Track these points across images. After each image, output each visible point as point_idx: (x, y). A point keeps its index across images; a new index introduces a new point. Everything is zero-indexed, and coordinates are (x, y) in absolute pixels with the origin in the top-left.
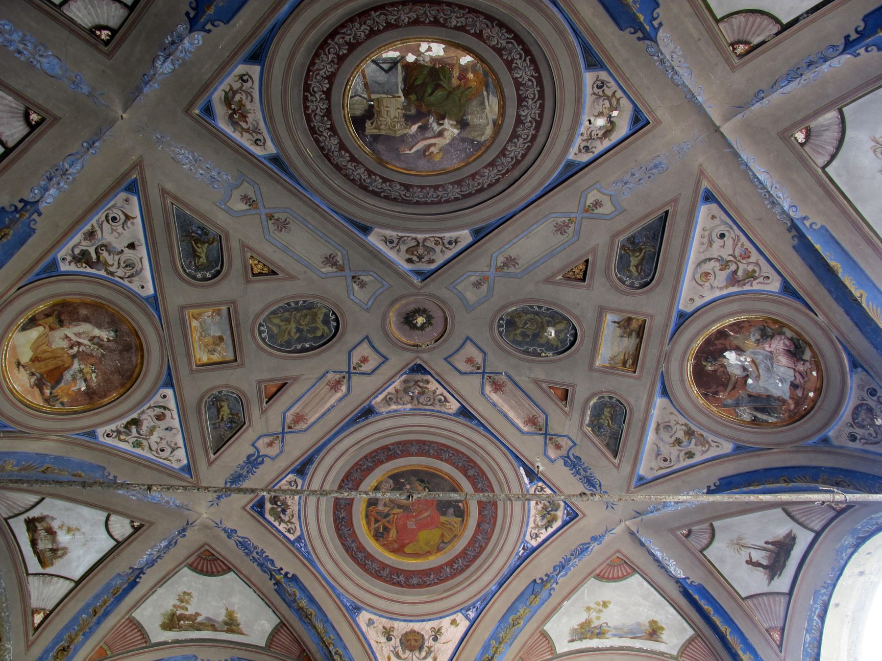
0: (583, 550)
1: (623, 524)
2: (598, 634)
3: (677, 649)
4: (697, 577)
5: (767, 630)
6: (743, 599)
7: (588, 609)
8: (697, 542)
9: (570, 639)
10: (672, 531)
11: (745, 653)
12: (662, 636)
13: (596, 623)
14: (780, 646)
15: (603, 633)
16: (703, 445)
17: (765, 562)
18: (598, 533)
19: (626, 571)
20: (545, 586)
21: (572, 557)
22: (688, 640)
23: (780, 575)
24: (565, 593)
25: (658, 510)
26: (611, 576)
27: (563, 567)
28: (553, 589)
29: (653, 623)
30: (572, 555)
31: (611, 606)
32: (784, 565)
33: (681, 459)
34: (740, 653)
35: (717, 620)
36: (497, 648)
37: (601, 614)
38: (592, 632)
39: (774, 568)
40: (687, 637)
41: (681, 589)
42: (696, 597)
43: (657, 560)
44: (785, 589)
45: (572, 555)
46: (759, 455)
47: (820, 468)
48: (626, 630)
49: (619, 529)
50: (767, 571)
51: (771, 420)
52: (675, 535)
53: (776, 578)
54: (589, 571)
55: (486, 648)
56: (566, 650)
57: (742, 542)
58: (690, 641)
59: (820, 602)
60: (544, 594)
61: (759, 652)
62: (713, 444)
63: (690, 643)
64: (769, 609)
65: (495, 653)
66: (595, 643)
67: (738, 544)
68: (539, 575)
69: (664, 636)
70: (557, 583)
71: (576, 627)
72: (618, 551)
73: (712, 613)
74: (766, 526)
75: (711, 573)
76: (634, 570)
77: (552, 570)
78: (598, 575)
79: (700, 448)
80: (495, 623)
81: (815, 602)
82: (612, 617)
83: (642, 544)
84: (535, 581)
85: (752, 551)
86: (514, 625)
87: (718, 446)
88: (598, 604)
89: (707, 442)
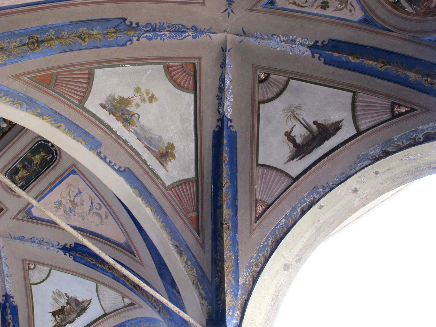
0: (179, 30)
1: (224, 35)
2: (126, 120)
3: (172, 181)
4: (238, 124)
5: (256, 201)
6: (258, 165)
7: (138, 90)
8: (264, 92)
9: (104, 102)
10: (255, 68)
11: (228, 208)
12: (169, 162)
13: (132, 108)
14: (257, 219)
15: (130, 123)
16: (341, 4)
17: (299, 141)
18: (201, 26)
19: (189, 84)
20: (129, 30)
21: (167, 29)
22: (186, 179)
23: (300, 159)
24: (136, 55)
25: (264, 39)
26: (175, 78)
27: (154, 30)
28: (131, 40)
29: (171, 146)
30: (169, 27)
31: (154, 104)
32: (311, 151)
33: (316, 5)
34: (225, 206)
35: (226, 170)
36: (52, 39)
37: (142, 104)
38: (123, 114)
39: (300, 150)
40: (187, 177)
41: (217, 129)
42: (225, 141)
43: (221, 89)
44: (294, 174)
45: (169, 27)
46: (378, 33)
47: (420, 60)
48: (148, 135)
49: (218, 37)
50: (295, 149)
51: (409, 9)
52: (254, 73)
53: (296, 159)
54: (167, 55)
55: (42, 30)
56: (92, 110)
57: (297, 112)
58: (186, 182)
59: (311, 198)
60: (123, 38)
61: (239, 214)
62: (349, 7)
63: (185, 183)
64: (270, 183)
65: (46, 41)
66: (116, 125)
67: (292, 112)
68: (132, 18)
69: (171, 164)
70: (138, 40)
71: (116, 97)
72: (199, 59)
73: (226, 162)
74: (327, 104)
75: (253, 126)
76: (195, 90)
77: (143, 25)
78: (169, 67)
79: (337, 4)
80: (67, 21)
81: (307, 197)
82: (148, 116)
83: (223, 65)
84: (125, 20)
85: (298, 124)
86: (80, 37)
87: (351, 11)
88: (147, 92)
89: (346, 3)
